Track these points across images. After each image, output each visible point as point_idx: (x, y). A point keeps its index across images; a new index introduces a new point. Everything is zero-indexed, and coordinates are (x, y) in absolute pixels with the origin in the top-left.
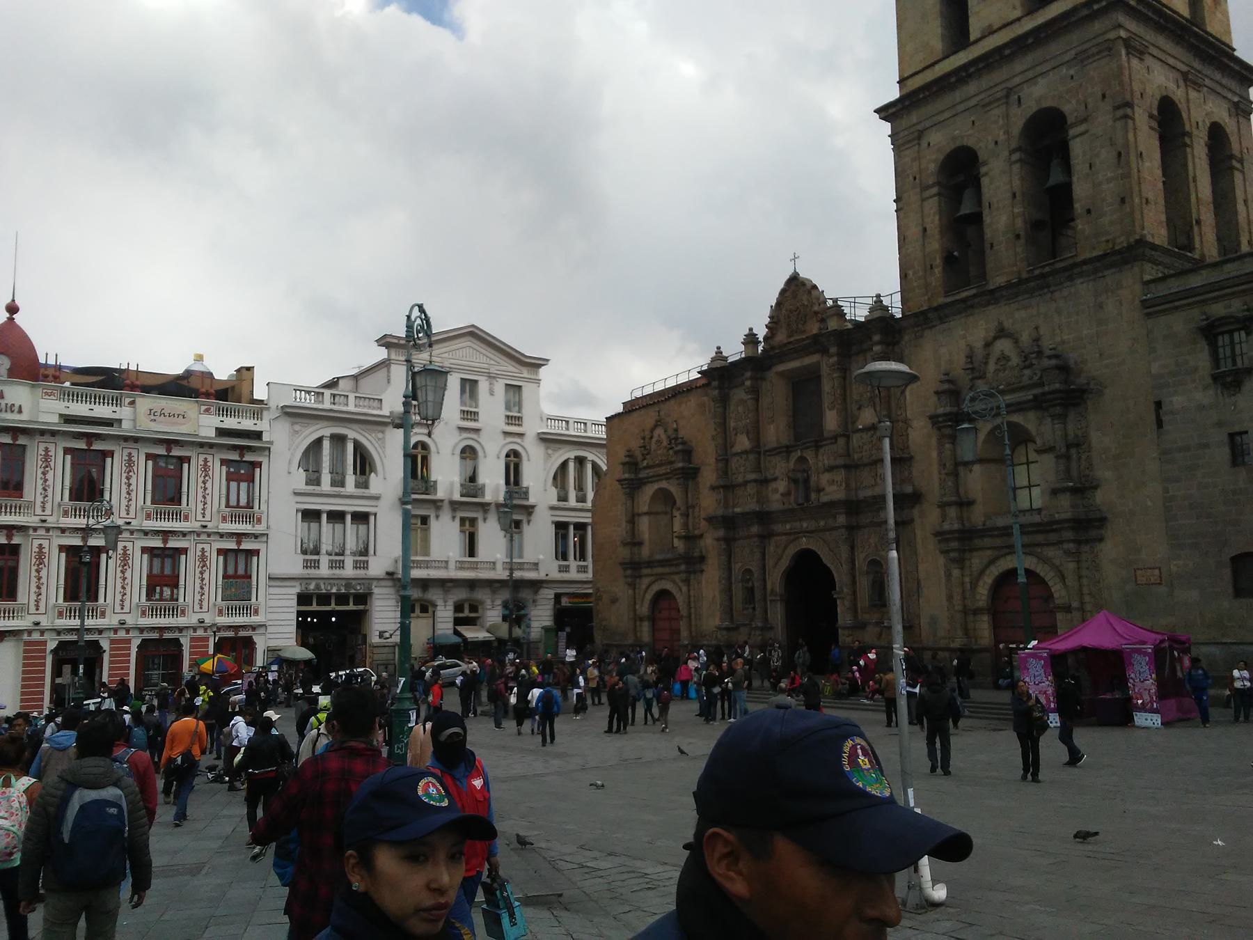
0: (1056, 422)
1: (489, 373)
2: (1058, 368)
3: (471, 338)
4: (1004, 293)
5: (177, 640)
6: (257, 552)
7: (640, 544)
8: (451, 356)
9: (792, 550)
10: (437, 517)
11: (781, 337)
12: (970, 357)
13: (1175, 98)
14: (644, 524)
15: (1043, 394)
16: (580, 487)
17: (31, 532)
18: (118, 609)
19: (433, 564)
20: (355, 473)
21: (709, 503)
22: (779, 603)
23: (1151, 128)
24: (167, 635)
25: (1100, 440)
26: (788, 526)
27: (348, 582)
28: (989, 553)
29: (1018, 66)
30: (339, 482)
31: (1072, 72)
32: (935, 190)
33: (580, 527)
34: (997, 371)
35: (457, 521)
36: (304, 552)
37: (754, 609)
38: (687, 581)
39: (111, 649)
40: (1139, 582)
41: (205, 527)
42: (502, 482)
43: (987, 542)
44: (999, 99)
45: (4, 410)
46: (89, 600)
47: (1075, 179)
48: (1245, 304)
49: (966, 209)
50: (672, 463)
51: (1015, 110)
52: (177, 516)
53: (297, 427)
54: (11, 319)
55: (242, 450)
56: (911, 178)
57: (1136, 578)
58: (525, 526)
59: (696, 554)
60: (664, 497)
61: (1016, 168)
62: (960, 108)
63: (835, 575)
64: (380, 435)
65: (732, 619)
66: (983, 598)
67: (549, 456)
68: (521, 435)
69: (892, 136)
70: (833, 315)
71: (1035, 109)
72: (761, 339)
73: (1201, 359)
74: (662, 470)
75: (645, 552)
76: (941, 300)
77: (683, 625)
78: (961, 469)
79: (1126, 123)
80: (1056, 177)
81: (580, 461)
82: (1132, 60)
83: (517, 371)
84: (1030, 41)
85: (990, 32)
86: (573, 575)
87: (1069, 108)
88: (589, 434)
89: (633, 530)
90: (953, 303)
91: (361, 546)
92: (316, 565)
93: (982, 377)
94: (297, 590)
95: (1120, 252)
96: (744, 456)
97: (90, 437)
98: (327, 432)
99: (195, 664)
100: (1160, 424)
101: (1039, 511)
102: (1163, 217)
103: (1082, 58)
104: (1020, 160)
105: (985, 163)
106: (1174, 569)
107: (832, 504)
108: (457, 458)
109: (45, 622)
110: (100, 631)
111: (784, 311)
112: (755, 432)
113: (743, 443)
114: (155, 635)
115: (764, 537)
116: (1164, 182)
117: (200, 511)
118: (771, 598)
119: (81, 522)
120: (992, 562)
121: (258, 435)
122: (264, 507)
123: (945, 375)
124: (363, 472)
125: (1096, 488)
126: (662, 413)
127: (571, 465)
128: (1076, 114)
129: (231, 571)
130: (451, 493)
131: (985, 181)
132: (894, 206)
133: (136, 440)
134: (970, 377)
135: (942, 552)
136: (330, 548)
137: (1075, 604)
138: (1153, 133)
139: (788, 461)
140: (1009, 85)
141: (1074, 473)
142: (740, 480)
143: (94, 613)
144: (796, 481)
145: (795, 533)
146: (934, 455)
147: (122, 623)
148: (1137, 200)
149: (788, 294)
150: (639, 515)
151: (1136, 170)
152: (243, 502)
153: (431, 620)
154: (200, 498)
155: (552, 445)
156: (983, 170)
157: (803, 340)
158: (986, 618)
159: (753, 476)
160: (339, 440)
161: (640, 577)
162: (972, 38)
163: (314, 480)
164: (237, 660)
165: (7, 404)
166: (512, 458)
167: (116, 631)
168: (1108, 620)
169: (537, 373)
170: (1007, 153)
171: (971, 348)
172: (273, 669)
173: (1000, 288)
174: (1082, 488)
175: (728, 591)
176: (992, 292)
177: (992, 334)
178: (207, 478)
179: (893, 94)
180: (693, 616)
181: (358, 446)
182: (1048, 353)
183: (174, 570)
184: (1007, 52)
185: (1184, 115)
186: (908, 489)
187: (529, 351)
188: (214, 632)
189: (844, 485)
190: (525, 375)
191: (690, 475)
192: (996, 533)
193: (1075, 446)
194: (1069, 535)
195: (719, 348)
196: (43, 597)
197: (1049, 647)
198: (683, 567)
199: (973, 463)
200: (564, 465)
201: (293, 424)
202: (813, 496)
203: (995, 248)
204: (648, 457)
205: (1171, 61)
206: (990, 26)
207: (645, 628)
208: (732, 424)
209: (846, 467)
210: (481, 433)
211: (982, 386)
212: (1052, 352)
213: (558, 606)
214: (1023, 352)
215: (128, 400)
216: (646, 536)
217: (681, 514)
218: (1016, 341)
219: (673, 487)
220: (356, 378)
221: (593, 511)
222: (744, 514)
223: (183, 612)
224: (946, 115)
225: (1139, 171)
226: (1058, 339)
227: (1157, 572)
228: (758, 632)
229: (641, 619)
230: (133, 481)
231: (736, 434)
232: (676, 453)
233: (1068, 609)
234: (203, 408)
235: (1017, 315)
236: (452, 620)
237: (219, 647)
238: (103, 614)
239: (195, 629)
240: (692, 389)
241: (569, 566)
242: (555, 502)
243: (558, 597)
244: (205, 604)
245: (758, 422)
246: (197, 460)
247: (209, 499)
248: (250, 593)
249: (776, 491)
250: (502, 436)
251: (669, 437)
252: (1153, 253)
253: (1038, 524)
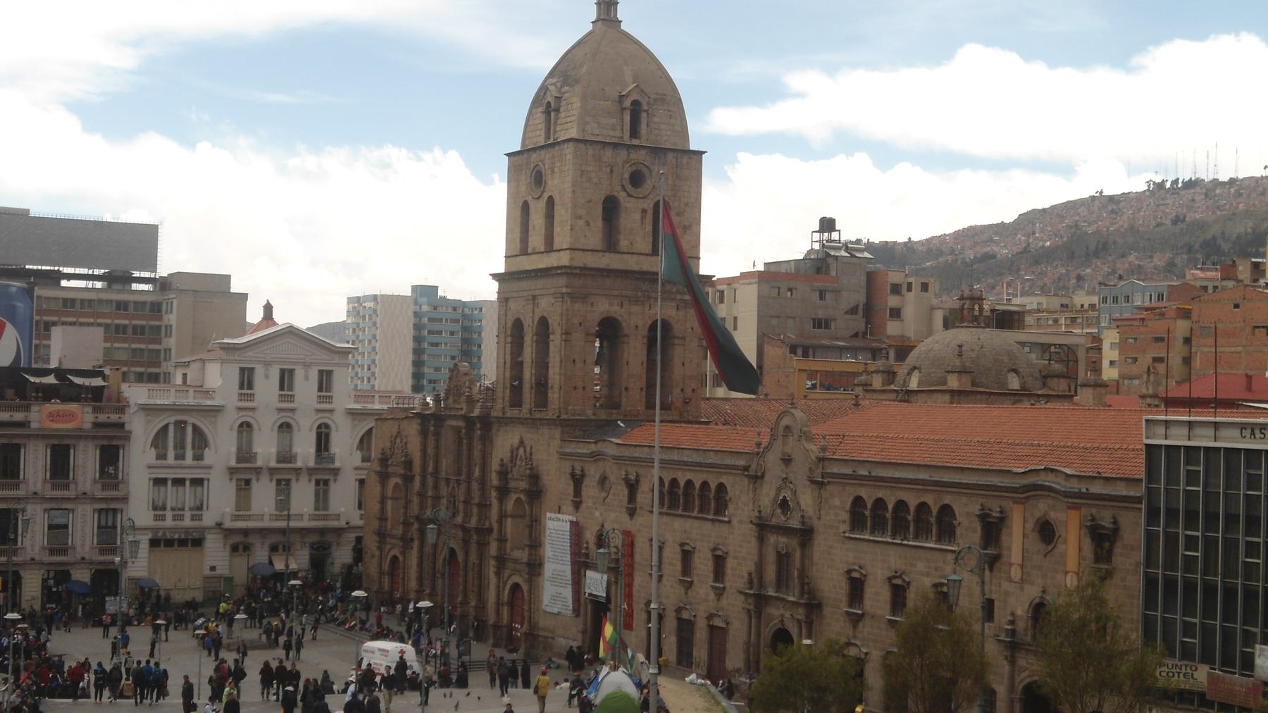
7: (386, 519)
10: (258, 480)
14: (389, 503)
27: (187, 530)
32: (509, 339)
36: (155, 508)
42: (312, 450)
48: (582, 467)
51: (536, 310)
58: (332, 484)
59: (409, 536)
64: (213, 419)
73: (571, 489)
83: (327, 358)
87: (550, 322)
92: (163, 518)
94: (150, 536)
98: (172, 420)
108: (275, 433)
129: (103, 523)
136: (174, 505)
160: (180, 425)
170: (531, 335)
175: (420, 564)
181: (195, 428)
184: (533, 274)
185: (624, 324)
190: (337, 361)
191: (408, 479)
205: (616, 293)
206: (534, 248)
207: (386, 580)
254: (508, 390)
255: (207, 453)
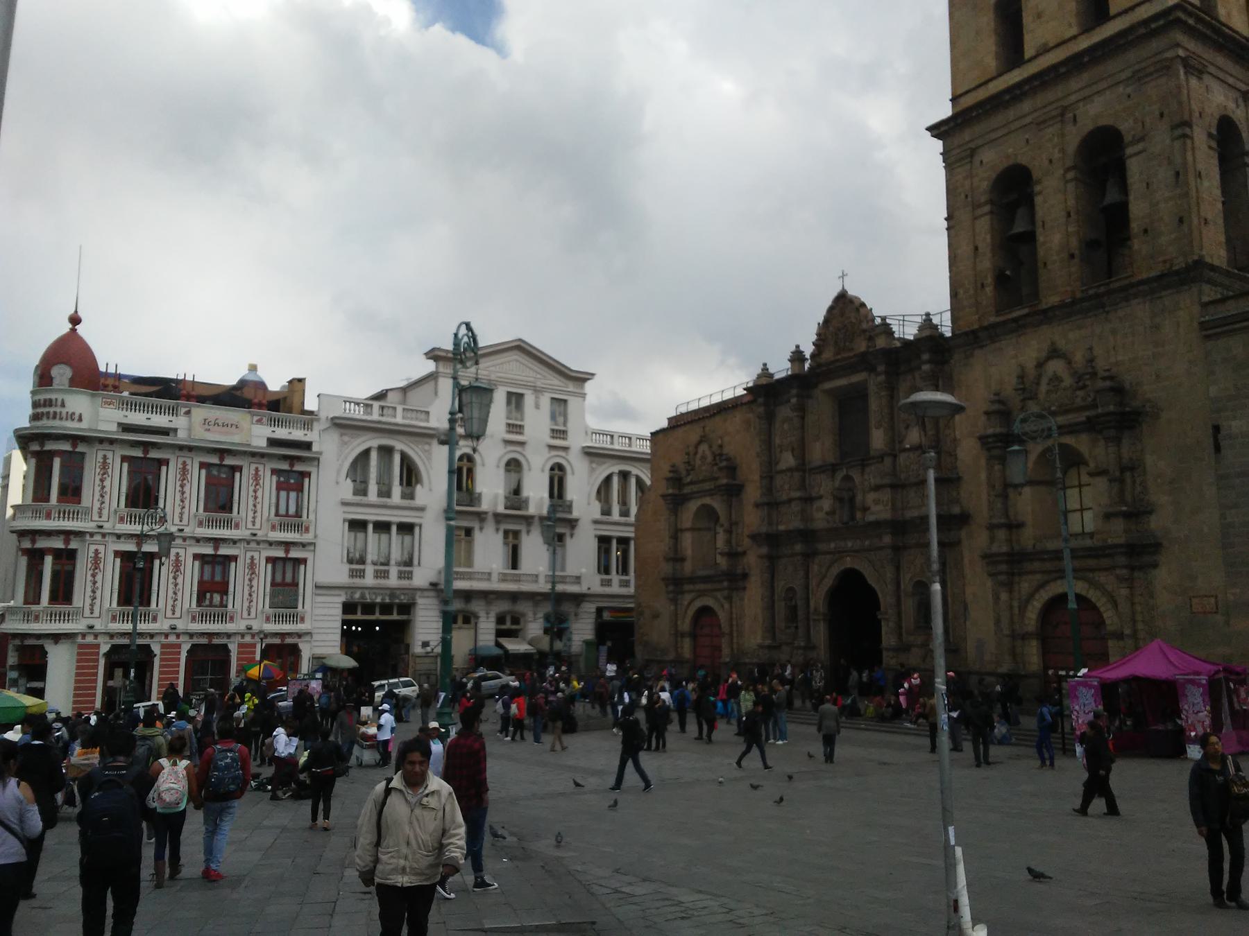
0: (1110, 444)
1: (535, 387)
2: (1112, 389)
3: (519, 353)
4: (1057, 313)
5: (225, 647)
6: (304, 561)
7: (683, 560)
8: (498, 369)
9: (836, 570)
10: (481, 529)
11: (828, 355)
12: (1021, 377)
13: (1234, 117)
14: (687, 540)
15: (1097, 416)
16: (624, 502)
17: (88, 537)
18: (169, 614)
19: (476, 576)
20: (401, 484)
21: (752, 519)
22: (822, 623)
23: (1210, 147)
24: (216, 641)
25: (1156, 463)
26: (832, 545)
27: (393, 592)
28: (1038, 576)
29: (1074, 84)
30: (385, 492)
31: (1129, 90)
32: (987, 208)
33: (623, 542)
34: (1048, 392)
35: (501, 535)
36: (350, 561)
37: (797, 628)
38: (729, 598)
39: (162, 653)
40: (1194, 610)
41: (255, 535)
42: (546, 495)
43: (1037, 565)
44: (1053, 117)
45: (65, 417)
46: (141, 604)
47: (1131, 198)
49: (1019, 227)
50: (716, 479)
52: (228, 524)
53: (346, 438)
54: (73, 330)
55: (292, 459)
56: (963, 196)
57: (1191, 606)
58: (568, 540)
59: (739, 571)
60: (708, 513)
61: (1071, 186)
62: (1013, 127)
63: (880, 595)
64: (427, 447)
65: (774, 637)
66: (1033, 622)
67: (592, 470)
68: (566, 449)
69: (945, 154)
70: (881, 334)
71: (1090, 126)
72: (808, 356)
74: (707, 486)
75: (688, 567)
76: (993, 319)
77: (724, 642)
78: (1011, 491)
79: (1185, 143)
80: (1112, 196)
81: (624, 475)
82: (1190, 78)
83: (562, 384)
84: (1086, 59)
85: (1045, 50)
86: (615, 589)
87: (1126, 126)
88: (634, 449)
89: (676, 544)
90: (1004, 322)
91: (406, 556)
92: (361, 574)
93: (1034, 397)
94: (343, 599)
95: (1177, 273)
96: (789, 474)
97: (146, 446)
99: (242, 670)
100: (1218, 448)
101: (1091, 535)
102: (1222, 239)
103: (1139, 77)
104: (1076, 179)
105: (1039, 182)
106: (1231, 598)
107: (877, 524)
108: (502, 471)
109: (99, 626)
110: (152, 636)
111: (831, 329)
112: (801, 450)
113: (788, 460)
114: (204, 641)
115: (809, 556)
116: (1224, 203)
117: (250, 519)
118: (816, 617)
119: (136, 528)
120: (1042, 586)
121: (307, 446)
122: (312, 517)
123: (995, 394)
124: (409, 483)
125: (1150, 513)
126: (707, 429)
127: (615, 480)
128: (1133, 133)
129: (279, 579)
130: (496, 504)
131: (1038, 200)
132: (945, 224)
133: (190, 449)
134: (1021, 398)
135: (991, 575)
136: (375, 558)
137: (1127, 631)
138: (1212, 153)
139: (833, 481)
140: (1065, 103)
141: (1128, 497)
142: (785, 497)
143: (146, 617)
144: (841, 500)
145: (839, 552)
146: (983, 476)
147: (173, 628)
148: (1195, 221)
149: (835, 311)
150: (682, 530)
151: (1194, 190)
152: (292, 510)
153: (472, 632)
154: (251, 506)
155: (596, 459)
156: (1037, 188)
157: (851, 358)
158: (1034, 643)
159: (798, 494)
160: (386, 451)
161: (682, 593)
162: (1027, 55)
163: (361, 491)
164: (282, 667)
165: (67, 413)
166: (556, 472)
167: (167, 636)
168: (1161, 648)
169: (582, 387)
171: (1023, 368)
172: (317, 676)
173: (1052, 308)
174: (1137, 513)
175: (770, 607)
176: (1045, 311)
177: (1044, 354)
178: (258, 487)
179: (945, 111)
180: (735, 635)
181: (405, 458)
182: (1101, 373)
183: (224, 579)
184: (1063, 70)
186: (956, 510)
187: (575, 365)
188: (262, 639)
189: (890, 504)
191: (733, 491)
192: (1046, 557)
193: (1129, 469)
194: (1122, 560)
195: (765, 365)
196: (98, 601)
197: (1100, 675)
198: (725, 584)
199: (1022, 485)
200: (608, 479)
201: (342, 435)
202: (859, 515)
203: (1049, 267)
204: (692, 472)
206: (1045, 44)
207: (687, 644)
208: (777, 441)
209: (894, 487)
210: (527, 447)
211: (1034, 408)
212: (1107, 374)
213: (599, 620)
214: (1076, 372)
215: (184, 410)
216: (689, 552)
217: (725, 531)
218: (1069, 363)
219: (717, 504)
220: (404, 390)
221: (637, 525)
222: (788, 532)
223: (232, 619)
224: (1000, 133)
225: (1197, 191)
226: (1113, 360)
227: (1212, 600)
228: (800, 652)
229: (683, 635)
230: (187, 489)
231: (781, 452)
232: (721, 469)
233: (1119, 636)
234: (256, 418)
235: (1071, 336)
236: (494, 631)
237: (266, 653)
238: (155, 619)
239: (243, 636)
240: (737, 405)
241: (611, 580)
242: (598, 516)
243: (599, 611)
244: (253, 611)
245: (803, 438)
246: (249, 469)
247: (259, 507)
248: (297, 600)
249: (820, 509)
250: (547, 449)
251: (713, 453)
252: (1212, 274)
253: (1090, 549)
254: (989, 290)
255: (419, 490)
